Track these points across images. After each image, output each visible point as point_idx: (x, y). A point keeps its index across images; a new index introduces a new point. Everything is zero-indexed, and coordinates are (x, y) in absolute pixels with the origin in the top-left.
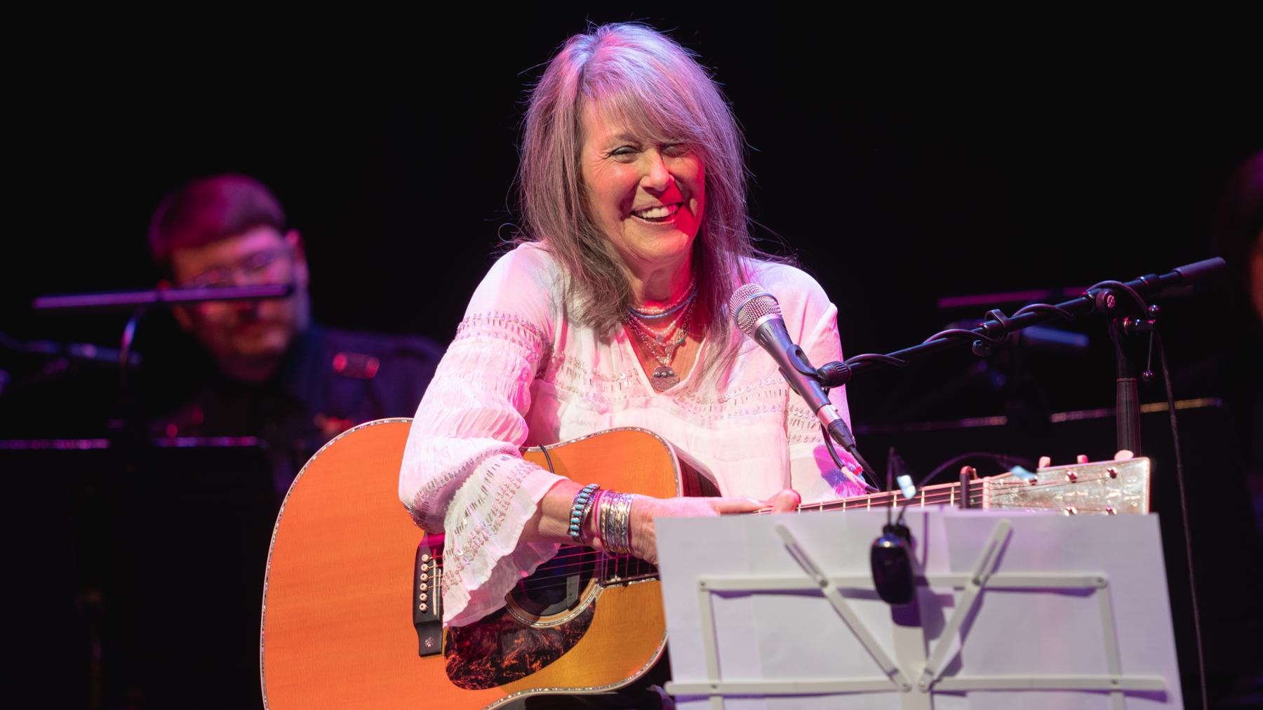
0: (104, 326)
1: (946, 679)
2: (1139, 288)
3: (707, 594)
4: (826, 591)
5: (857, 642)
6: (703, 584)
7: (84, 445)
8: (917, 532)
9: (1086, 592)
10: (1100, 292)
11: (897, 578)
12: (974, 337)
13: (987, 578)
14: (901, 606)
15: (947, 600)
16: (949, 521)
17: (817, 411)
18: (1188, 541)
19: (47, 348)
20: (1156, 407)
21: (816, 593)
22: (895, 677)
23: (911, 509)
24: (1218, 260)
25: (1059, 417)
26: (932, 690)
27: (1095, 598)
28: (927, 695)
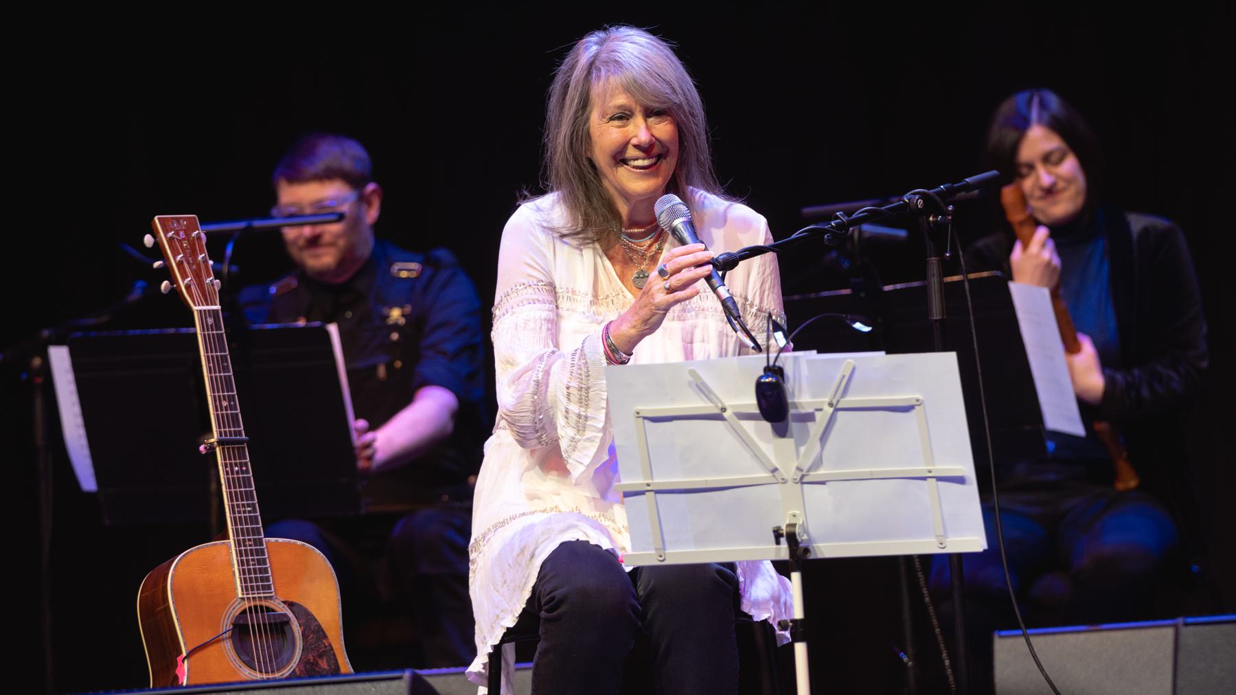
4: (726, 415)
8: (789, 371)
9: (907, 409)
10: (913, 198)
11: (773, 403)
12: (826, 231)
15: (809, 417)
16: (809, 362)
17: (714, 290)
20: (956, 278)
21: (718, 417)
24: (994, 172)
25: (887, 288)
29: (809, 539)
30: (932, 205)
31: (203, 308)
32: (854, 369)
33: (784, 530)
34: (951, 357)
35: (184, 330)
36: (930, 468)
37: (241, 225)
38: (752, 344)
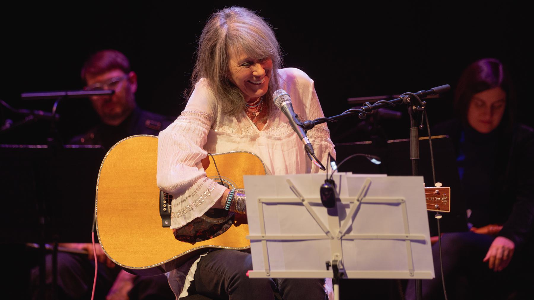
0: (47, 103)
1: (347, 235)
2: (420, 95)
3: (261, 204)
4: (304, 203)
6: (260, 200)
7: (39, 147)
8: (337, 182)
9: (397, 204)
10: (405, 97)
11: (329, 198)
12: (360, 112)
13: (362, 199)
14: (330, 209)
15: (348, 206)
16: (348, 178)
19: (25, 111)
21: (300, 204)
22: (328, 234)
27: (400, 206)
28: (340, 241)
29: (343, 269)
34: (421, 179)
36: (408, 235)
38: (320, 166)
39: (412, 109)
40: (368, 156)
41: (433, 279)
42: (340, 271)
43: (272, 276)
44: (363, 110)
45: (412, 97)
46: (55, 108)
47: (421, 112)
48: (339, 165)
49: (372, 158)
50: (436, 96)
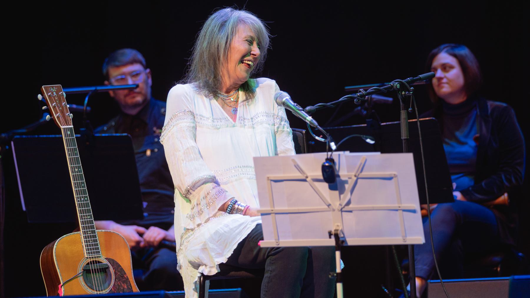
2: (408, 82)
4: (308, 179)
5: (317, 195)
8: (336, 160)
9: (390, 179)
10: (396, 84)
11: (330, 175)
14: (332, 184)
15: (346, 182)
16: (346, 157)
18: (424, 162)
21: (304, 180)
22: (330, 207)
23: (334, 153)
25: (382, 124)
26: (342, 211)
27: (393, 180)
28: (340, 212)
29: (344, 237)
30: (403, 87)
31: (66, 127)
32: (366, 160)
33: (333, 232)
35: (58, 136)
36: (400, 205)
37: (93, 88)
39: (402, 94)
40: (363, 137)
41: (424, 244)
42: (341, 239)
43: (282, 245)
44: (358, 96)
45: (402, 84)
46: (86, 102)
47: (409, 97)
48: (338, 145)
49: (367, 138)
50: (423, 83)
